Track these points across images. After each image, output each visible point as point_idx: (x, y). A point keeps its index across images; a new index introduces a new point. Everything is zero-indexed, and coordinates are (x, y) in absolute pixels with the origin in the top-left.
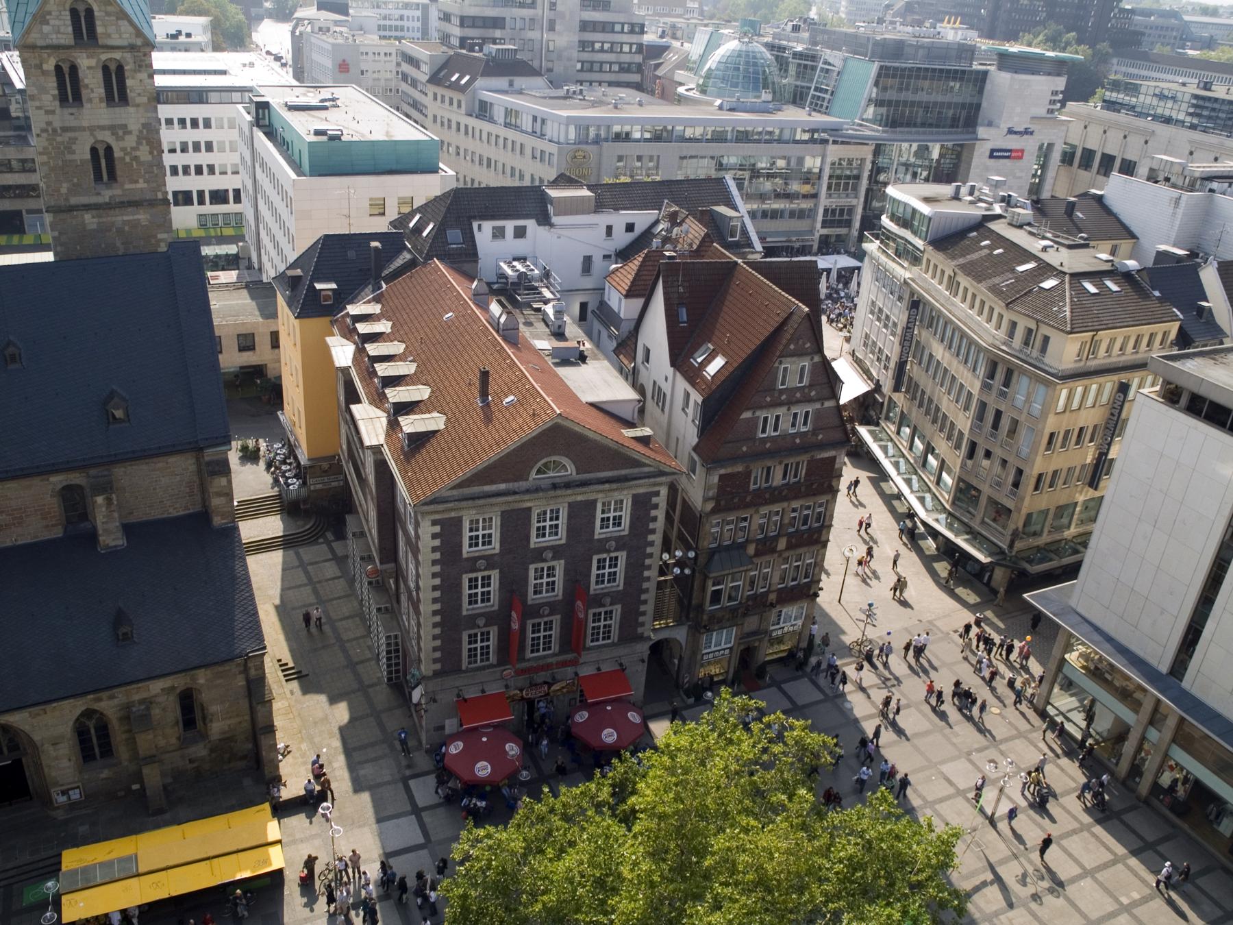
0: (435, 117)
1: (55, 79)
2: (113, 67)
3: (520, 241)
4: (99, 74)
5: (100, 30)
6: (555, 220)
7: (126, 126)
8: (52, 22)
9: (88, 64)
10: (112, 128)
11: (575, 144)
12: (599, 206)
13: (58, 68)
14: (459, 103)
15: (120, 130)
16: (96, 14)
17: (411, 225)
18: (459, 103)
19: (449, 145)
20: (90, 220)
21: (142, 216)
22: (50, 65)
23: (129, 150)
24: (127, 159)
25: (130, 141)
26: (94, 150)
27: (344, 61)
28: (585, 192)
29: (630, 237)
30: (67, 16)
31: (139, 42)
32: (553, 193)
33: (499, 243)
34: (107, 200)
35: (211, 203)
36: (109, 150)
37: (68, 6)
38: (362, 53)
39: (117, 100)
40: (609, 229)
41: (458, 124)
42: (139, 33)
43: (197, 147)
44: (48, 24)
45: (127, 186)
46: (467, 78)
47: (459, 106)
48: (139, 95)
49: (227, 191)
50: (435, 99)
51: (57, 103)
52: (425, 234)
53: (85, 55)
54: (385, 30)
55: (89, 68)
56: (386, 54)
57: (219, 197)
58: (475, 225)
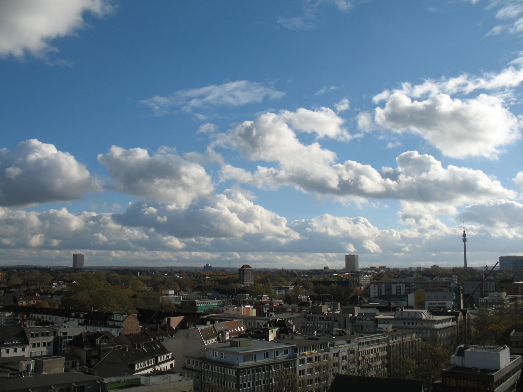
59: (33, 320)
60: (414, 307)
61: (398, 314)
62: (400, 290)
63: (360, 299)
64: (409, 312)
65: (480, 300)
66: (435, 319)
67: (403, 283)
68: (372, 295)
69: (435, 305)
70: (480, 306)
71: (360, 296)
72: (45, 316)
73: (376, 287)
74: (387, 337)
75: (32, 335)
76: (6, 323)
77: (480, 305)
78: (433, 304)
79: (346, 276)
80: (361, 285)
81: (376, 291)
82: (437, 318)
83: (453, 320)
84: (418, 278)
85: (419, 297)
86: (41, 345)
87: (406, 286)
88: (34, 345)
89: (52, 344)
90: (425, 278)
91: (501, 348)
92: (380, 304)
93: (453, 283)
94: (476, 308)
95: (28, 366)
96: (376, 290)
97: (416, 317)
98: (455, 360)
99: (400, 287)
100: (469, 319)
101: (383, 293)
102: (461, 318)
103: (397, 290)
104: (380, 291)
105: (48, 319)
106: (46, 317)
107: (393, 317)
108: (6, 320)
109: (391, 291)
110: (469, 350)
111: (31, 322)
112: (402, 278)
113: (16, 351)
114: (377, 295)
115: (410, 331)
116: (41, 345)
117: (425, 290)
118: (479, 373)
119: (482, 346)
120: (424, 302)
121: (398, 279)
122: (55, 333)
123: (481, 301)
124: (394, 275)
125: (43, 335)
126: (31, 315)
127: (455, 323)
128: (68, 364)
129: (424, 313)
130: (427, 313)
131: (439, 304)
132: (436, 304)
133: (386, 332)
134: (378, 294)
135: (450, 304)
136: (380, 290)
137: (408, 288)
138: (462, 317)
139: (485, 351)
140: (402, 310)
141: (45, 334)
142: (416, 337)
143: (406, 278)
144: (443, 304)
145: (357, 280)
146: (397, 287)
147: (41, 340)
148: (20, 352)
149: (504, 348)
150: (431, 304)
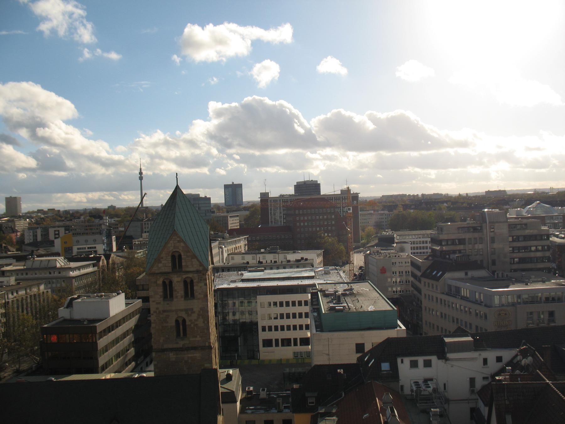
0: (425, 295)
1: (162, 287)
2: (188, 281)
3: (428, 370)
4: (182, 285)
5: (183, 264)
6: (450, 356)
7: (192, 309)
8: (163, 262)
9: (177, 280)
10: (186, 310)
11: (499, 307)
12: (477, 346)
13: (164, 283)
14: (437, 286)
15: (189, 311)
16: (183, 257)
17: (366, 359)
18: (437, 286)
19: (433, 310)
20: (172, 356)
21: (197, 355)
22: (160, 282)
23: (193, 321)
24: (192, 325)
25: (194, 316)
26: (177, 321)
27: (383, 267)
28: (470, 339)
29: (499, 365)
30: (169, 258)
31: (201, 268)
32: (447, 340)
33: (414, 370)
34: (181, 346)
35: (301, 345)
36: (184, 321)
37: (170, 254)
38: (393, 263)
39: (190, 296)
40: (485, 361)
41: (437, 298)
42: (201, 265)
43: (294, 316)
44: (161, 263)
45: (191, 339)
46: (441, 273)
47: (437, 289)
48: (200, 294)
49: (272, 340)
50: (425, 285)
51: (162, 299)
52: (369, 365)
53: (176, 276)
54: (414, 249)
55: (178, 282)
56: (406, 262)
57: (305, 341)
58: (399, 360)
60: (61, 254)
61: (29, 264)
62: (58, 234)
63: (5, 247)
64: (41, 261)
65: (134, 241)
66: (70, 267)
67: (62, 227)
68: (27, 241)
69: (85, 250)
70: (134, 248)
71: (5, 244)
73: (30, 232)
74: (3, 292)
77: (133, 247)
78: (83, 248)
79: (4, 221)
80: (17, 231)
81: (31, 237)
82: (73, 265)
83: (94, 265)
84: (85, 220)
85: (65, 243)
87: (66, 230)
90: (93, 219)
91: (114, 295)
92: (21, 253)
93: (104, 225)
94: (126, 250)
96: (31, 236)
97: (49, 266)
98: (63, 313)
99: (58, 231)
100: (114, 263)
101: (39, 238)
102: (103, 263)
103: (55, 234)
104: (35, 237)
107: (22, 267)
109: (49, 236)
110: (79, 300)
112: (68, 221)
114: (32, 241)
115: (30, 283)
117: (73, 234)
118: (85, 324)
119: (95, 294)
120: (72, 247)
121: (64, 222)
123: (135, 242)
124: (59, 218)
127: (96, 269)
129: (59, 261)
130: (63, 261)
131: (88, 248)
132: (85, 248)
133: (7, 286)
134: (34, 239)
135: (101, 248)
136: (35, 236)
137: (67, 232)
138: (105, 262)
139: (95, 300)
140: (34, 258)
142: (45, 289)
143: (72, 221)
144: (93, 248)
145: (11, 226)
146: (55, 231)
149: (118, 294)
150: (80, 249)
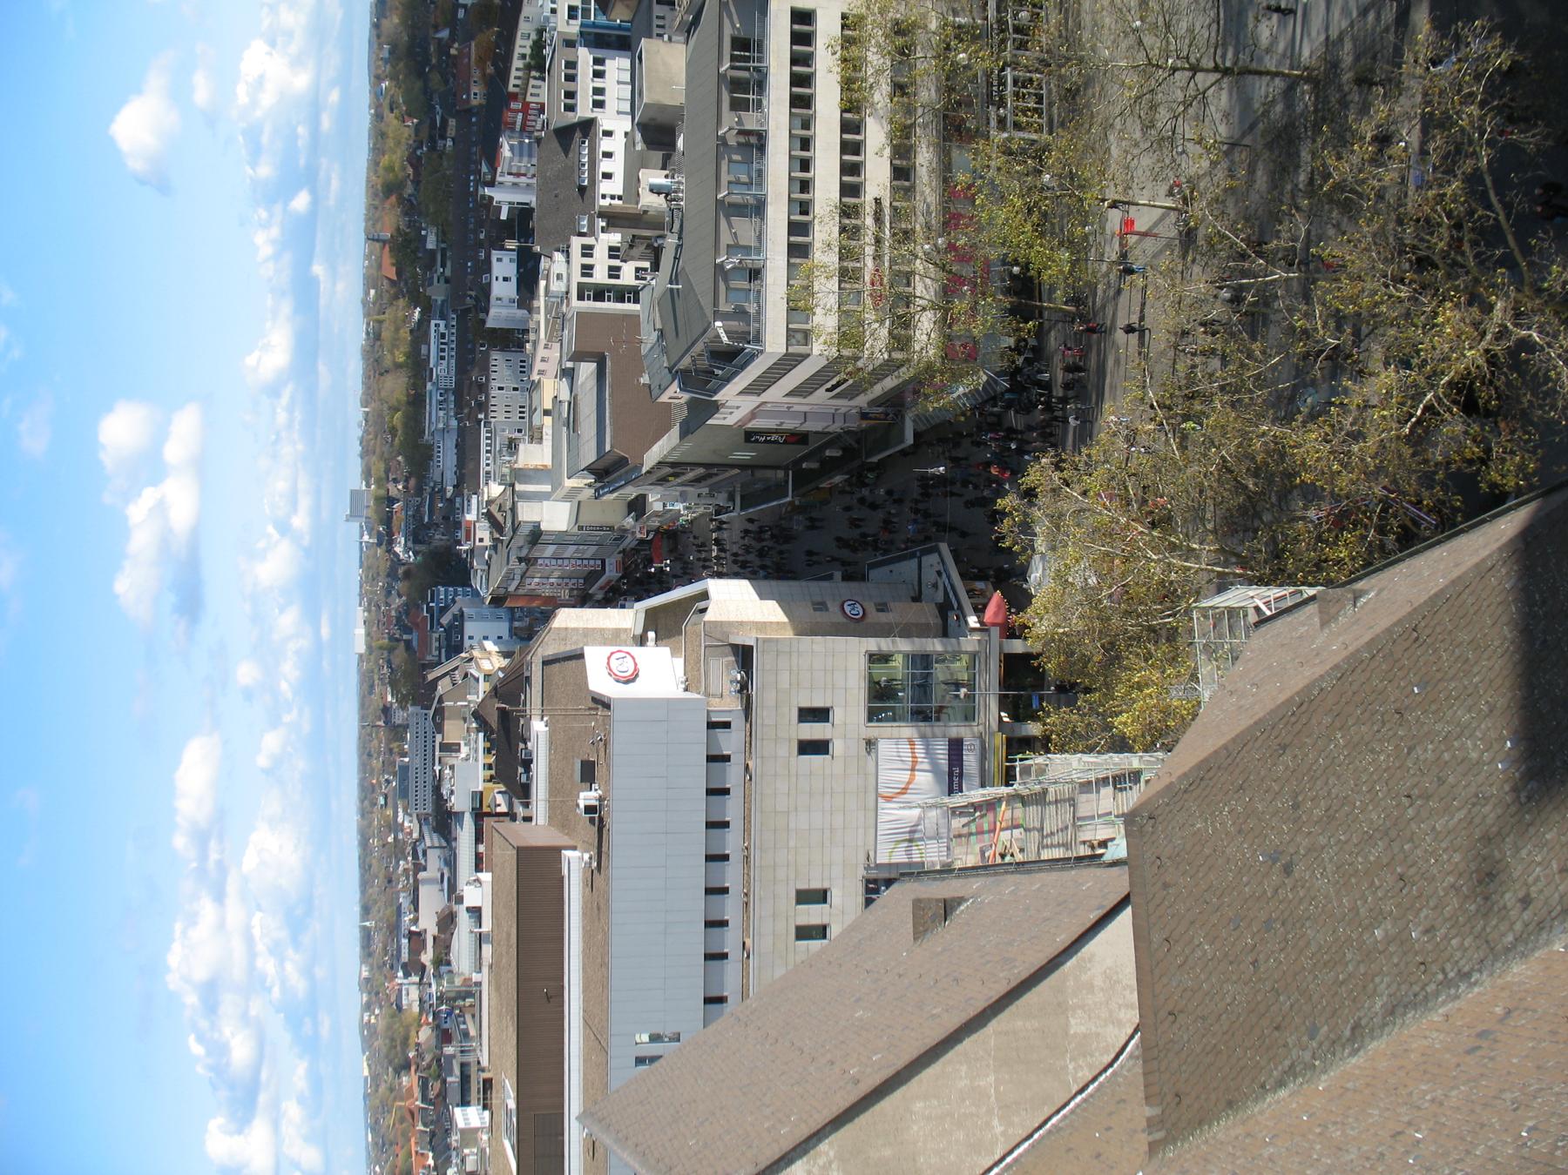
59: (527, 84)
72: (518, 51)
75: (570, 108)
76: (530, 156)
86: (599, 83)
88: (599, 104)
89: (600, 54)
95: (655, 190)
105: (529, 43)
106: (522, 46)
108: (521, 155)
111: (531, 90)
113: (608, 155)
116: (599, 83)
122: (570, 44)
125: (571, 78)
126: (511, 89)
128: (663, 18)
141: (571, 71)
147: (585, 84)
148: (616, 145)
